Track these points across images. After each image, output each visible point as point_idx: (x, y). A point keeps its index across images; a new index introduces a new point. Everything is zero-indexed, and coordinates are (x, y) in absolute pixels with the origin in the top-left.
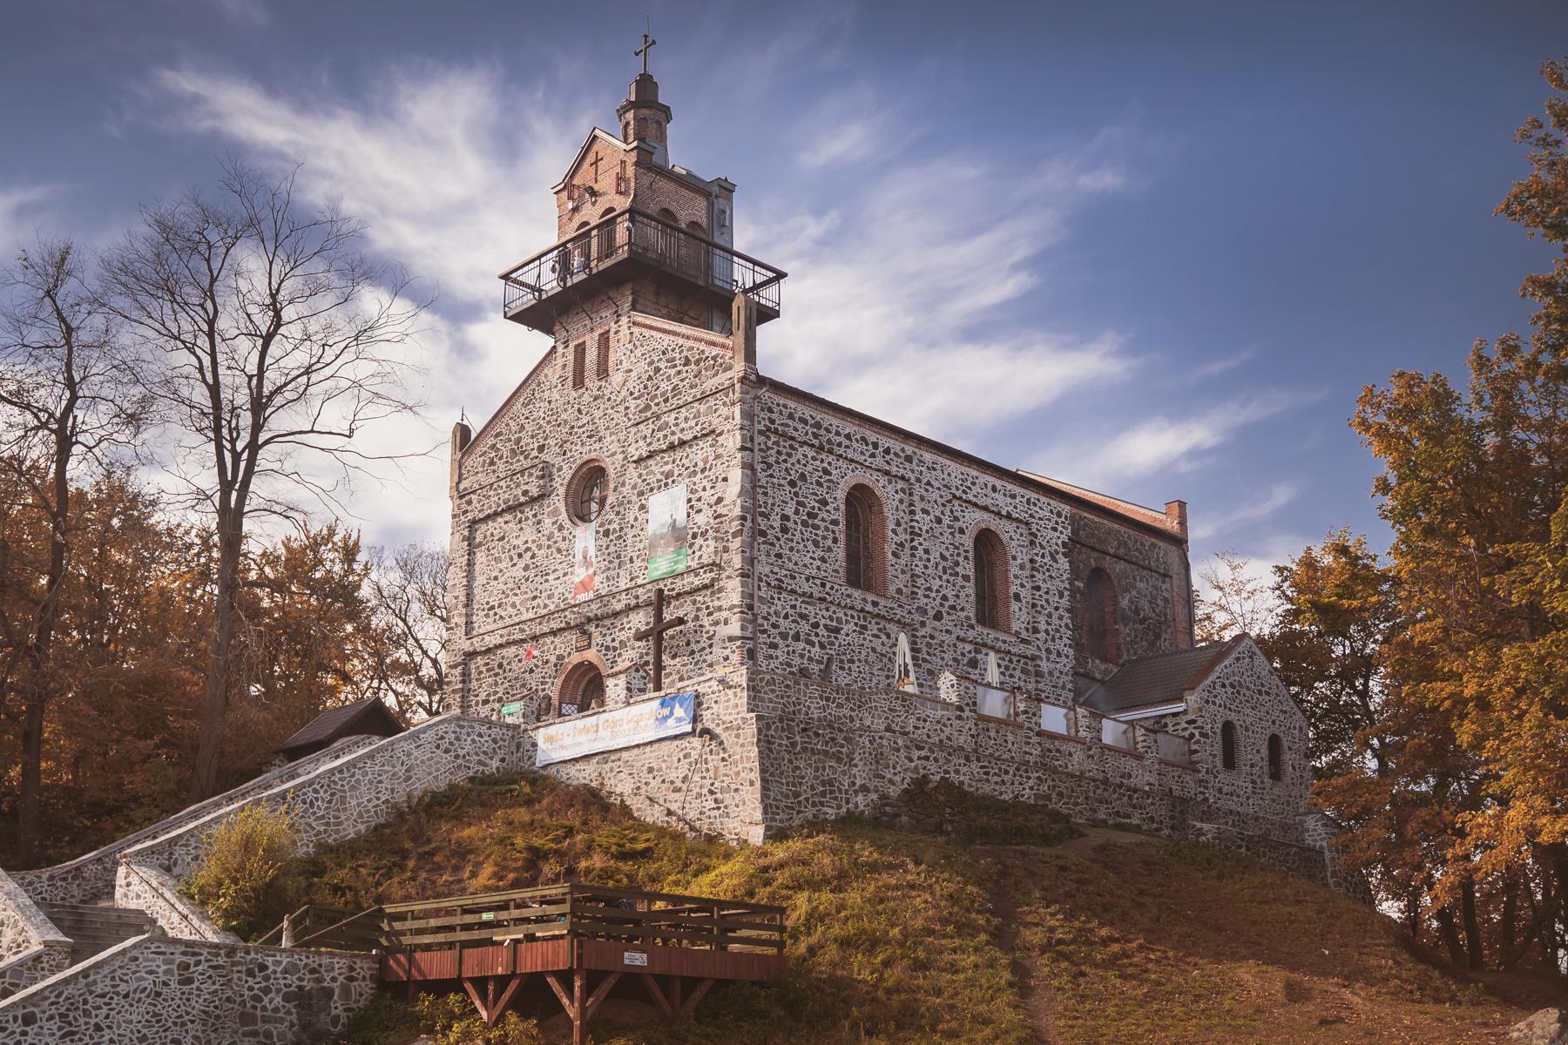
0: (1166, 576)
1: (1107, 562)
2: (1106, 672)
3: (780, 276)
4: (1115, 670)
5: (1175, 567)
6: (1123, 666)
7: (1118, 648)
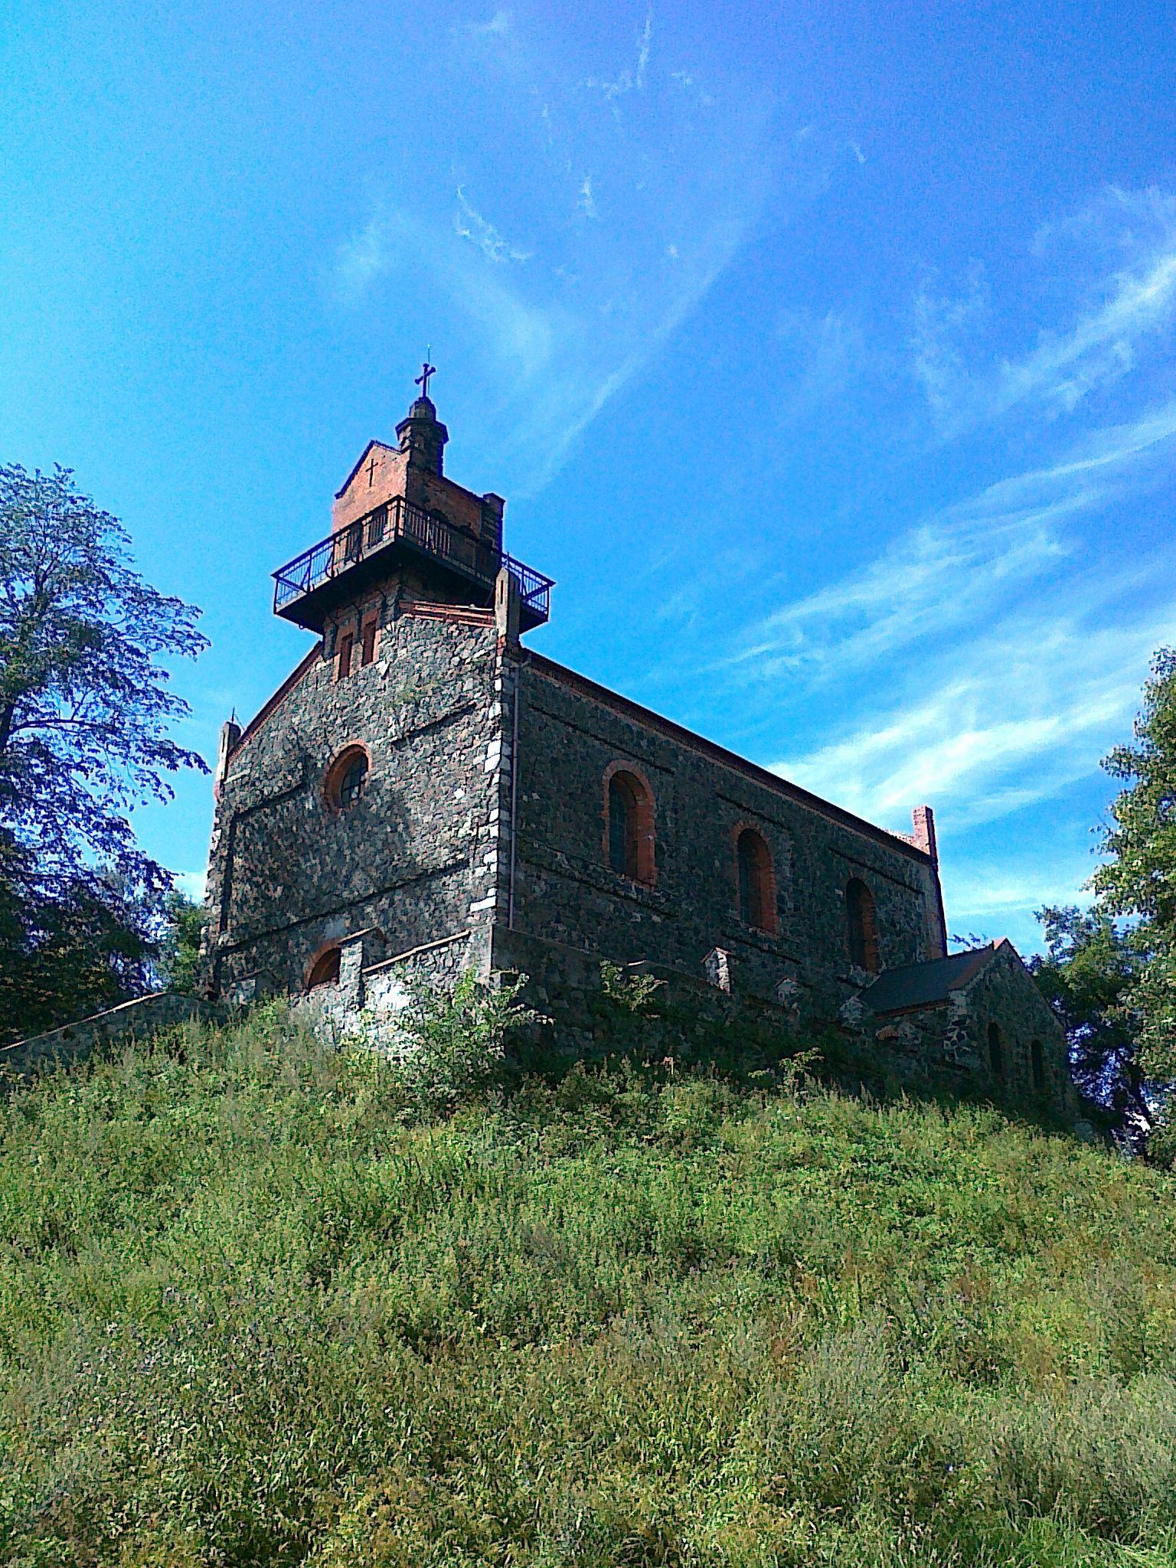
0: (918, 892)
1: (865, 874)
2: (867, 980)
3: (551, 583)
4: (876, 978)
5: (928, 885)
6: (882, 974)
7: (878, 957)
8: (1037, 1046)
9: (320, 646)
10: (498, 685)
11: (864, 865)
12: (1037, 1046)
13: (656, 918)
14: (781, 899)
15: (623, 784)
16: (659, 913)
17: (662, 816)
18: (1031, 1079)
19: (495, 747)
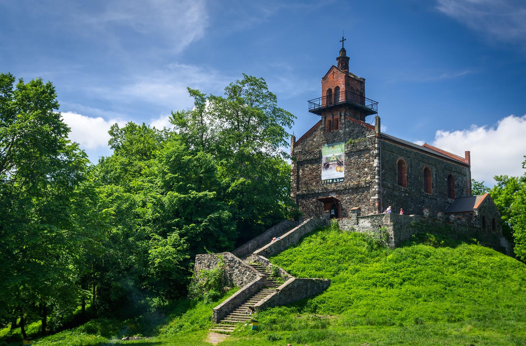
0: (465, 175)
2: (452, 201)
3: (377, 103)
5: (468, 173)
6: (455, 199)
7: (454, 195)
8: (494, 220)
9: (321, 121)
10: (376, 146)
12: (494, 220)
13: (407, 195)
14: (433, 184)
15: (401, 162)
16: (407, 193)
17: (408, 169)
18: (492, 229)
19: (376, 161)
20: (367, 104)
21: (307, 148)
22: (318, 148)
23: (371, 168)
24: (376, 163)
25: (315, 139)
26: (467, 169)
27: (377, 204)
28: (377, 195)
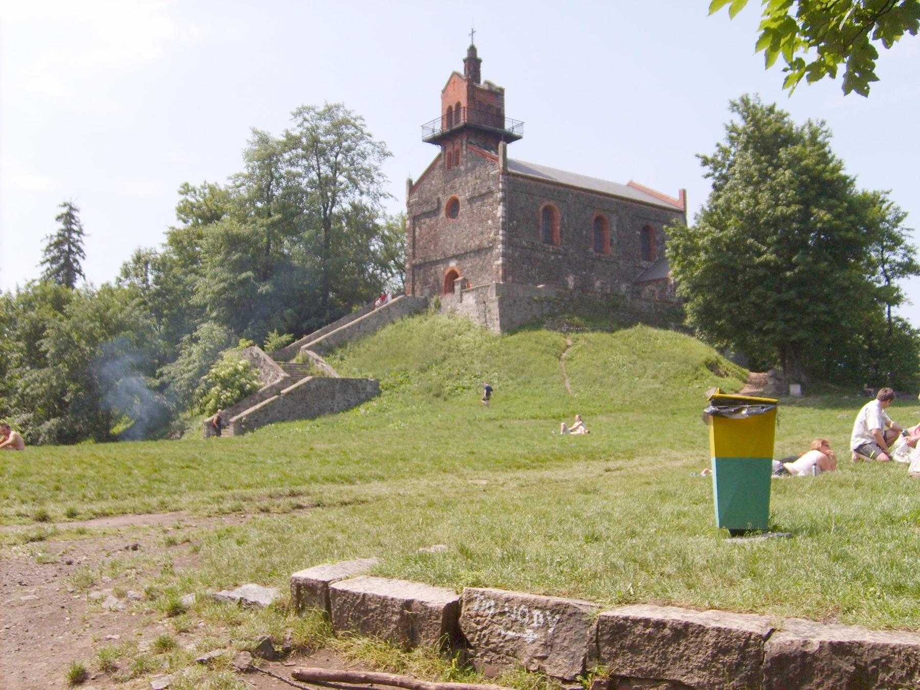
10: (501, 186)
11: (650, 219)
13: (560, 257)
14: (612, 240)
15: (548, 211)
17: (563, 219)
20: (508, 126)
21: (424, 196)
22: (437, 194)
23: (494, 218)
24: (500, 211)
25: (433, 182)
26: (680, 216)
27: (501, 272)
28: (501, 258)
